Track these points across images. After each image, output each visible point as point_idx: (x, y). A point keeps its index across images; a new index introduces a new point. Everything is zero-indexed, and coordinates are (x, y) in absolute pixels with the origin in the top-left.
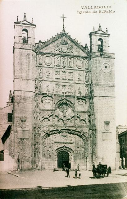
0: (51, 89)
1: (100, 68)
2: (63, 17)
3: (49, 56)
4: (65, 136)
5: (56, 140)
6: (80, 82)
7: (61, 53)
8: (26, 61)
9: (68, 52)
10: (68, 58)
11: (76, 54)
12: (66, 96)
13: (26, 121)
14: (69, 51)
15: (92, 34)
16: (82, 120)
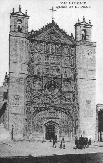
0: (41, 72)
1: (83, 54)
2: (53, 10)
3: (40, 43)
4: (52, 113)
5: (44, 116)
6: (66, 66)
7: (50, 41)
8: (20, 47)
9: (56, 41)
10: (56, 45)
11: (63, 41)
12: (54, 78)
13: (19, 99)
14: (57, 40)
15: (77, 25)
16: (67, 99)
